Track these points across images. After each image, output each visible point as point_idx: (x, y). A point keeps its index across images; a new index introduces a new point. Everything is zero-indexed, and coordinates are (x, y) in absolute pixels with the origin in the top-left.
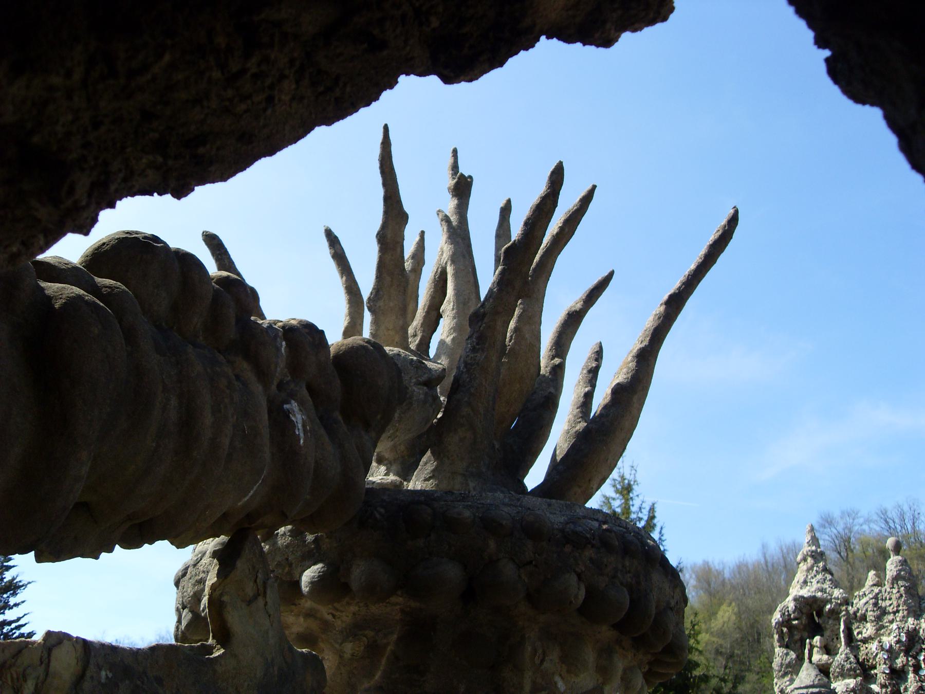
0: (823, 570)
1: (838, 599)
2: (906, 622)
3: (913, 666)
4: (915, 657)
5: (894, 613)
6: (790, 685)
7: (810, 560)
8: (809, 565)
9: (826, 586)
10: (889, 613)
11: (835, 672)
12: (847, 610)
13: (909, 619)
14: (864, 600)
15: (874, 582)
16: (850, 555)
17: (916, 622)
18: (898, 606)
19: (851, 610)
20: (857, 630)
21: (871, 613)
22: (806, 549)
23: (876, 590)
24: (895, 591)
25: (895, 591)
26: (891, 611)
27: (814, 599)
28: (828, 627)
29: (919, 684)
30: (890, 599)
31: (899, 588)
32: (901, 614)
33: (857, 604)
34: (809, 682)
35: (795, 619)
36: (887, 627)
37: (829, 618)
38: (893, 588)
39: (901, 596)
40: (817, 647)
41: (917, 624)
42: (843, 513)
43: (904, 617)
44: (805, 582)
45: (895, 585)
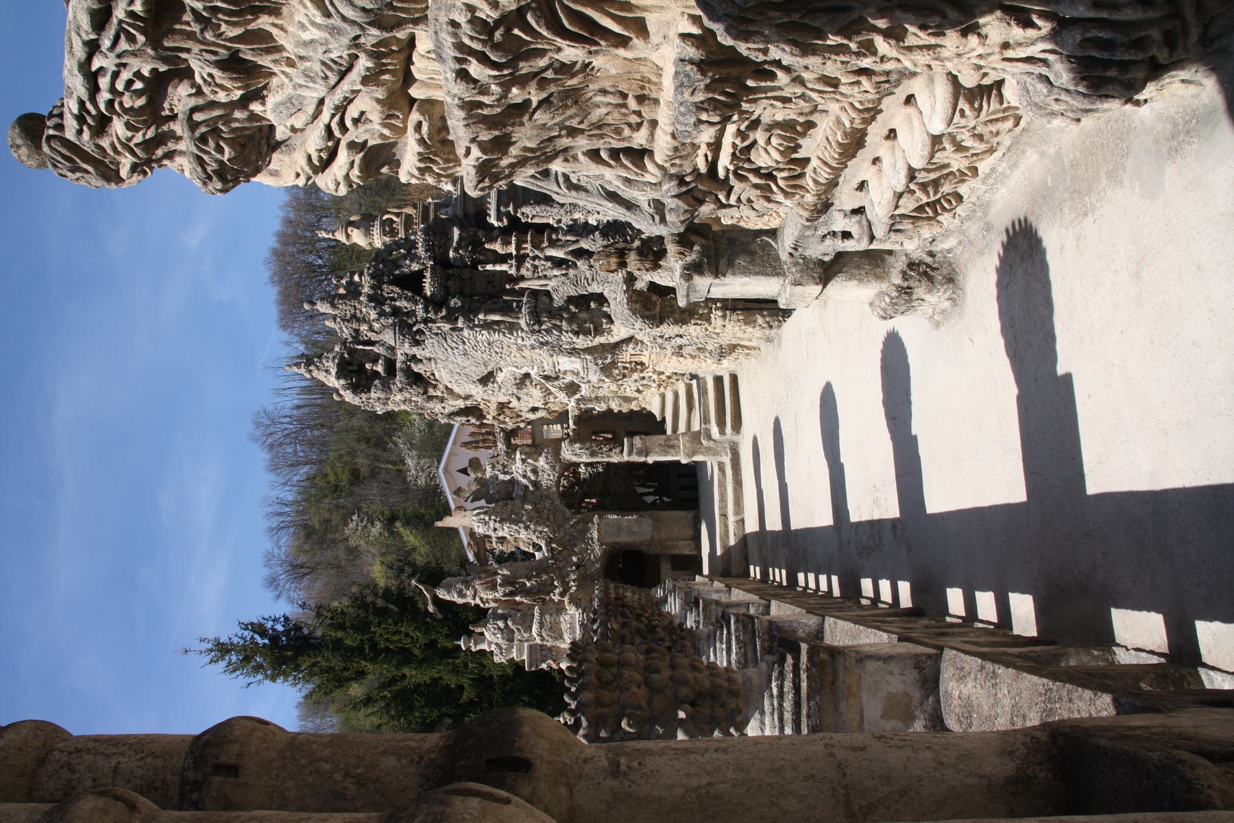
4: (386, 299)
5: (355, 309)
7: (311, 368)
9: (331, 356)
12: (350, 343)
14: (344, 329)
16: (307, 565)
19: (350, 339)
22: (302, 370)
23: (338, 320)
42: (266, 566)
44: (327, 371)
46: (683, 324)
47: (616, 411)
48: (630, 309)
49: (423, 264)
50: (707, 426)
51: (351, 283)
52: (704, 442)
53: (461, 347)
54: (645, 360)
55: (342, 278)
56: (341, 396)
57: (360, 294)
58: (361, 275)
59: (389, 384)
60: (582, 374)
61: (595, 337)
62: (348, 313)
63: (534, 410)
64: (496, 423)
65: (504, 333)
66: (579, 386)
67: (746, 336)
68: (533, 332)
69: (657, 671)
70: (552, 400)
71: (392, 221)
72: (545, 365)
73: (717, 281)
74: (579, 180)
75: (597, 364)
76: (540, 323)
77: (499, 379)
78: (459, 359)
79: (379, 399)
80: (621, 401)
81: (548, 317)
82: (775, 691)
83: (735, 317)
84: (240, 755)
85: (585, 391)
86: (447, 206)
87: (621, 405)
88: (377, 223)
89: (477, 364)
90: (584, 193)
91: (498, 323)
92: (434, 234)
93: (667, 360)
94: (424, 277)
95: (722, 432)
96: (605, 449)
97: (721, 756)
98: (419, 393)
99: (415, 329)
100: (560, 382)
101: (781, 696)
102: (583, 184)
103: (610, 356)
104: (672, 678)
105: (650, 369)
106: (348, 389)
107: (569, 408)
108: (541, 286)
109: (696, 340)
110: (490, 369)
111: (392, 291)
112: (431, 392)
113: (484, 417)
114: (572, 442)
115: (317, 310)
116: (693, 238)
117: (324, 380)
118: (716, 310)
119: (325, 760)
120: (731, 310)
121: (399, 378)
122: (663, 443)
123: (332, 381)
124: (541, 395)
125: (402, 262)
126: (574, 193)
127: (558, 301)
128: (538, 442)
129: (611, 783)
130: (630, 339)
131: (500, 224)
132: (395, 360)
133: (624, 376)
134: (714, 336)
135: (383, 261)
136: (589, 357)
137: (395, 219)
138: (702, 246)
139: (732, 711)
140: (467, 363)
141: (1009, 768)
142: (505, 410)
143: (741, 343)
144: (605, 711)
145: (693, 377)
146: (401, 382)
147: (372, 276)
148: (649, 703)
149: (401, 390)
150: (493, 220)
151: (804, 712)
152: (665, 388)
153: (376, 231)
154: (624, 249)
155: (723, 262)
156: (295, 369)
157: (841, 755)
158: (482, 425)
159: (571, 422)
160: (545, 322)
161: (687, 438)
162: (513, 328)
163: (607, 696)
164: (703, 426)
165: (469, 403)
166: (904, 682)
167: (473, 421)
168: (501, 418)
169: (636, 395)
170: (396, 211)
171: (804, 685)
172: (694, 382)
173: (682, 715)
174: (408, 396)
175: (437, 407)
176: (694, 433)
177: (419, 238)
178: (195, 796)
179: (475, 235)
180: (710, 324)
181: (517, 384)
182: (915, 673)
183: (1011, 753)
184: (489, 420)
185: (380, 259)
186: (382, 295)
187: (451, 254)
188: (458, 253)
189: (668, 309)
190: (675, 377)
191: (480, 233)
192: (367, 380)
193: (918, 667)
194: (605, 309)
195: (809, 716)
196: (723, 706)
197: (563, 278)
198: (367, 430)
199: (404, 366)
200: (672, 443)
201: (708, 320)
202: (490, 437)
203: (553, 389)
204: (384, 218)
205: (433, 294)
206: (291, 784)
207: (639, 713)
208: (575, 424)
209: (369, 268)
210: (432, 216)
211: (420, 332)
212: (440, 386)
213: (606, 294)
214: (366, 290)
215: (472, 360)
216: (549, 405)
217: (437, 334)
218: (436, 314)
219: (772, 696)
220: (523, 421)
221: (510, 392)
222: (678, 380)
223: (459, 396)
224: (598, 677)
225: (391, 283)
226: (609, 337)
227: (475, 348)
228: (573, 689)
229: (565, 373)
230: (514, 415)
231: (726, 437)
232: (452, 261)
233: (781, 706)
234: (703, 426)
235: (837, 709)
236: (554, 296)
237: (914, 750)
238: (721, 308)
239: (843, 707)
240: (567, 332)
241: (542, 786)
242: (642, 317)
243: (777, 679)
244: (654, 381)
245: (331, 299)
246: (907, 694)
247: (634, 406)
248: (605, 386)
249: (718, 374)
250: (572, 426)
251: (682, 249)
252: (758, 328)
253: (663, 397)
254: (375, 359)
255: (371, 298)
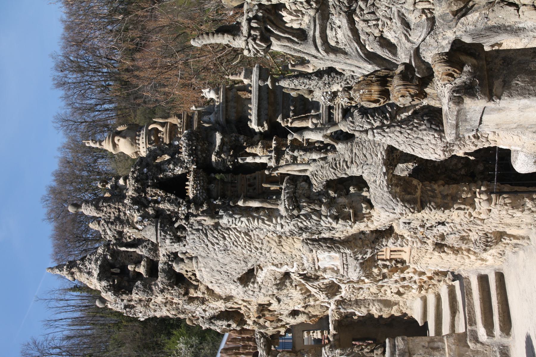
0: (83, 261)
1: (104, 251)
2: (126, 204)
3: (155, 204)
4: (149, 202)
5: (119, 211)
6: (158, 286)
7: (73, 270)
8: (77, 270)
9: (93, 258)
10: (119, 215)
11: (153, 255)
12: (113, 245)
13: (125, 202)
14: (108, 231)
15: (97, 223)
17: (127, 198)
18: (115, 208)
19: (114, 241)
20: (128, 239)
21: (117, 227)
22: (65, 273)
23: (103, 222)
24: (105, 209)
25: (105, 209)
26: (117, 214)
27: (101, 267)
28: (122, 261)
29: (166, 201)
30: (110, 213)
31: (104, 206)
32: (121, 207)
33: (110, 237)
34: (153, 229)
35: (114, 281)
36: (128, 217)
37: (116, 259)
38: (103, 211)
39: (109, 206)
40: (135, 268)
41: (129, 197)
43: (123, 205)
44: (89, 273)
45: (101, 209)
46: (446, 208)
47: (376, 316)
48: (390, 192)
49: (186, 168)
50: (473, 328)
51: (116, 186)
52: (471, 345)
53: (221, 243)
54: (405, 256)
55: (107, 183)
56: (103, 301)
57: (124, 197)
58: (126, 178)
59: (150, 285)
60: (341, 272)
61: (355, 222)
62: (112, 215)
63: (294, 313)
64: (256, 328)
65: (263, 220)
66: (339, 287)
67: (513, 221)
68: (292, 217)
70: (312, 303)
71: (157, 131)
72: (305, 262)
73: (491, 105)
74: (337, 42)
75: (356, 259)
76: (299, 208)
77: (259, 280)
78: (220, 256)
79: (140, 300)
80: (382, 306)
81: (307, 202)
83: (501, 201)
85: (345, 292)
86: (210, 113)
87: (381, 310)
88: (143, 132)
89: (237, 261)
90: (342, 56)
91: (257, 209)
92: (197, 139)
93: (428, 256)
94: (187, 180)
95: (490, 333)
96: (366, 350)
98: (181, 294)
99: (176, 225)
100: (320, 283)
102: (341, 46)
103: (370, 251)
105: (410, 270)
106: (109, 290)
107: (329, 312)
108: (300, 171)
109: (459, 227)
110: (250, 266)
111: (156, 194)
112: (193, 293)
113: (245, 323)
114: (333, 347)
115: (82, 214)
116: (463, 58)
117: (86, 282)
118: (480, 194)
120: (496, 193)
121: (161, 278)
122: (427, 345)
123: (95, 284)
124: (301, 297)
125: (165, 167)
126: (332, 56)
127: (317, 185)
128: (298, 348)
130: (389, 232)
131: (261, 129)
132: (157, 262)
133: (384, 276)
134: (479, 222)
135: (147, 165)
136: (348, 252)
137: (160, 128)
138: (473, 66)
140: (228, 259)
142: (266, 313)
143: (509, 232)
145: (457, 277)
146: (162, 283)
147: (137, 180)
149: (162, 291)
150: (254, 126)
152: (427, 290)
153: (142, 141)
154: (387, 76)
155: (497, 84)
156: (57, 272)
158: (243, 331)
159: (331, 327)
160: (304, 207)
161: (452, 340)
162: (272, 214)
164: (469, 327)
165: (229, 305)
167: (234, 326)
168: (261, 321)
169: (397, 298)
170: (161, 121)
172: (457, 283)
174: (169, 296)
175: (198, 310)
176: (459, 334)
177: (183, 143)
179: (237, 140)
180: (475, 209)
181: (277, 285)
184: (250, 325)
185: (144, 163)
186: (145, 198)
187: (214, 158)
188: (220, 157)
189: (429, 193)
190: (436, 278)
191: (242, 138)
192: (128, 281)
194: (364, 194)
197: (322, 163)
198: (128, 333)
199: (166, 267)
200: (436, 345)
201: (473, 205)
202: (251, 343)
203: (313, 291)
204: (150, 128)
205: (195, 197)
208: (335, 329)
209: (133, 172)
210: (195, 126)
211: (182, 228)
212: (202, 287)
213: (365, 177)
214: (130, 193)
215: (232, 256)
216: (310, 309)
217: (198, 230)
218: (197, 209)
220: (283, 326)
221: (270, 293)
222: (439, 281)
223: (220, 297)
225: (154, 186)
226: (369, 223)
227: (235, 243)
229: (325, 270)
230: (274, 318)
231: (495, 339)
232: (214, 165)
234: (469, 327)
236: (314, 182)
238: (485, 192)
240: (326, 217)
242: (402, 201)
244: (415, 282)
245: (96, 203)
247: (395, 311)
248: (365, 286)
249: (483, 273)
250: (332, 331)
251: (451, 70)
252: (527, 212)
253: (425, 300)
254: (137, 260)
255: (135, 201)
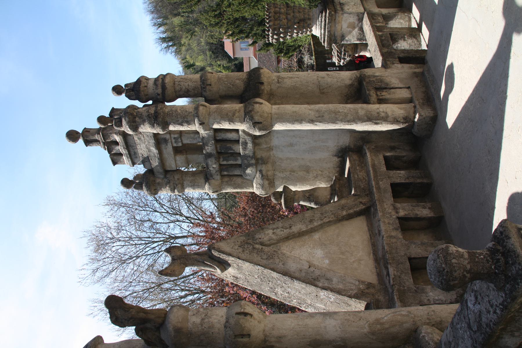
69: (289, 14)
82: (320, 20)
84: (211, 82)
97: (297, 79)
101: (321, 22)
104: (293, 16)
119: (226, 81)
129: (278, 84)
139: (309, 24)
141: (350, 82)
144: (276, 27)
148: (287, 24)
151: (327, 27)
157: (320, 79)
163: (277, 22)
166: (354, 19)
171: (327, 21)
173: (295, 26)
178: (204, 90)
182: (357, 17)
183: (351, 79)
193: (358, 16)
195: (328, 28)
196: (306, 23)
206: (220, 86)
207: (285, 27)
219: (319, 21)
224: (274, 17)
228: (268, 21)
233: (321, 24)
235: (335, 26)
237: (333, 79)
239: (337, 26)
241: (266, 86)
243: (321, 18)
246: (354, 22)
